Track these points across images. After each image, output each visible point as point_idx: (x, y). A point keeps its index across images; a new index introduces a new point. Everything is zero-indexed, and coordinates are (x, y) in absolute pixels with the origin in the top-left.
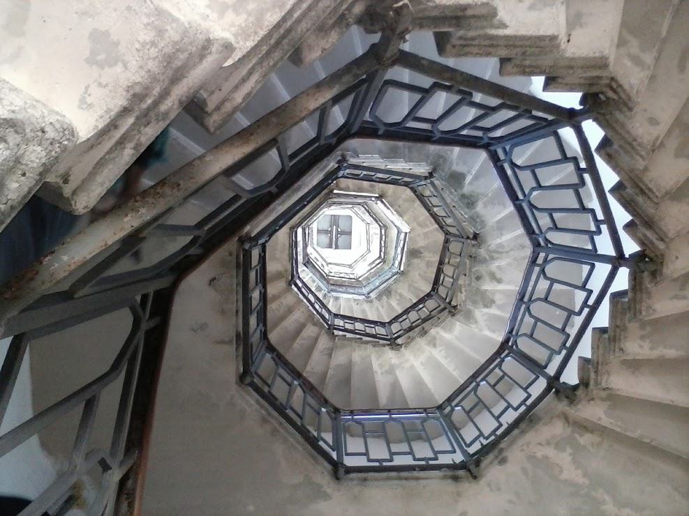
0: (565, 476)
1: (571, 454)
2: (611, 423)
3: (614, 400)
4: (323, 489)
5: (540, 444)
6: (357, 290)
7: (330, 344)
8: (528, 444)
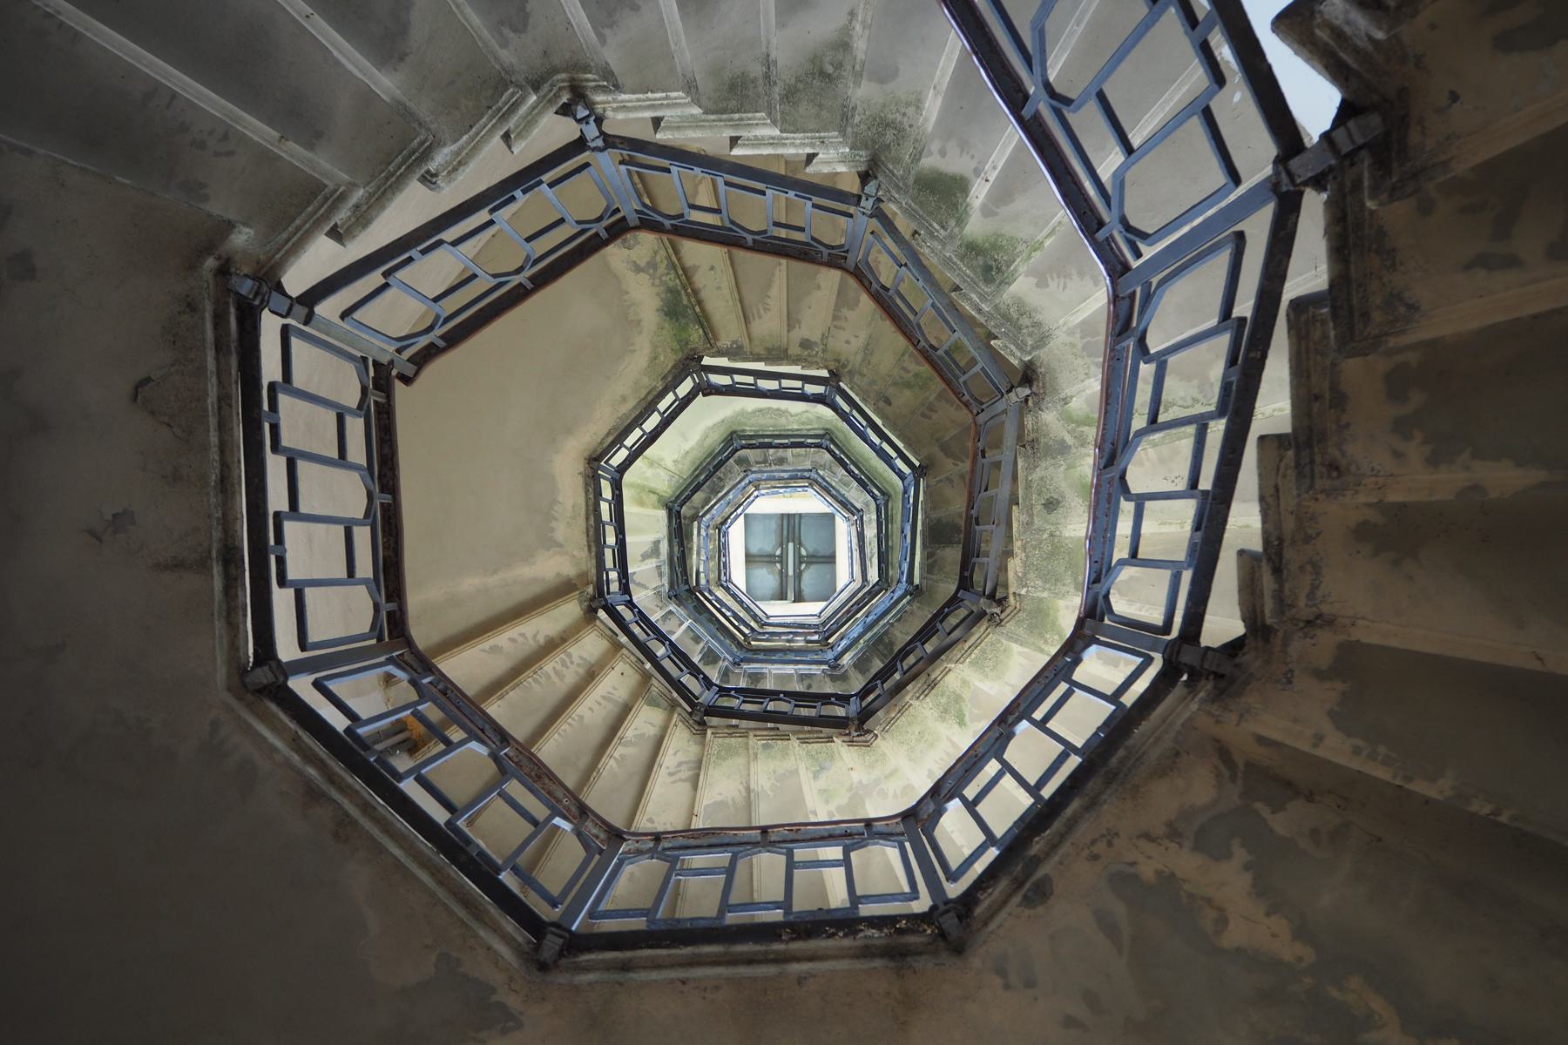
0: (1235, 936)
4: (494, 998)
5: (1147, 836)
7: (694, 749)
8: (1111, 837)
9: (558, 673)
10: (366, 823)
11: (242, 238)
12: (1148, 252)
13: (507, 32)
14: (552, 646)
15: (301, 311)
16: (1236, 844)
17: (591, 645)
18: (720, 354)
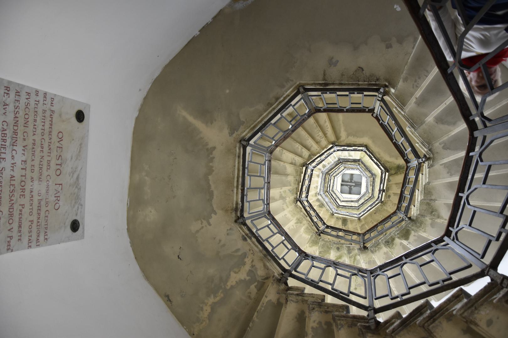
0: (233, 274)
1: (245, 279)
2: (263, 304)
3: (278, 307)
5: (252, 261)
6: (322, 188)
7: (298, 164)
8: (253, 254)
9: (319, 134)
10: (271, 109)
11: (393, 90)
12: (372, 278)
13: (442, 145)
14: (325, 134)
15: (380, 99)
16: (250, 278)
17: (324, 142)
18: (388, 177)
